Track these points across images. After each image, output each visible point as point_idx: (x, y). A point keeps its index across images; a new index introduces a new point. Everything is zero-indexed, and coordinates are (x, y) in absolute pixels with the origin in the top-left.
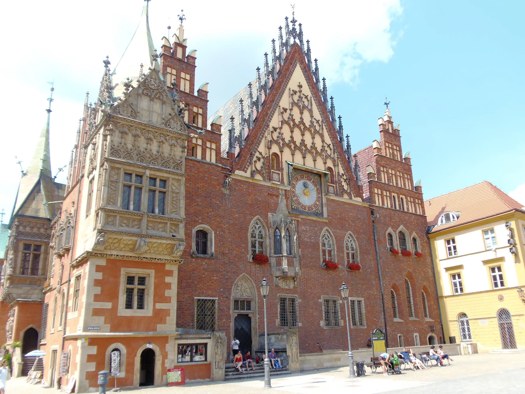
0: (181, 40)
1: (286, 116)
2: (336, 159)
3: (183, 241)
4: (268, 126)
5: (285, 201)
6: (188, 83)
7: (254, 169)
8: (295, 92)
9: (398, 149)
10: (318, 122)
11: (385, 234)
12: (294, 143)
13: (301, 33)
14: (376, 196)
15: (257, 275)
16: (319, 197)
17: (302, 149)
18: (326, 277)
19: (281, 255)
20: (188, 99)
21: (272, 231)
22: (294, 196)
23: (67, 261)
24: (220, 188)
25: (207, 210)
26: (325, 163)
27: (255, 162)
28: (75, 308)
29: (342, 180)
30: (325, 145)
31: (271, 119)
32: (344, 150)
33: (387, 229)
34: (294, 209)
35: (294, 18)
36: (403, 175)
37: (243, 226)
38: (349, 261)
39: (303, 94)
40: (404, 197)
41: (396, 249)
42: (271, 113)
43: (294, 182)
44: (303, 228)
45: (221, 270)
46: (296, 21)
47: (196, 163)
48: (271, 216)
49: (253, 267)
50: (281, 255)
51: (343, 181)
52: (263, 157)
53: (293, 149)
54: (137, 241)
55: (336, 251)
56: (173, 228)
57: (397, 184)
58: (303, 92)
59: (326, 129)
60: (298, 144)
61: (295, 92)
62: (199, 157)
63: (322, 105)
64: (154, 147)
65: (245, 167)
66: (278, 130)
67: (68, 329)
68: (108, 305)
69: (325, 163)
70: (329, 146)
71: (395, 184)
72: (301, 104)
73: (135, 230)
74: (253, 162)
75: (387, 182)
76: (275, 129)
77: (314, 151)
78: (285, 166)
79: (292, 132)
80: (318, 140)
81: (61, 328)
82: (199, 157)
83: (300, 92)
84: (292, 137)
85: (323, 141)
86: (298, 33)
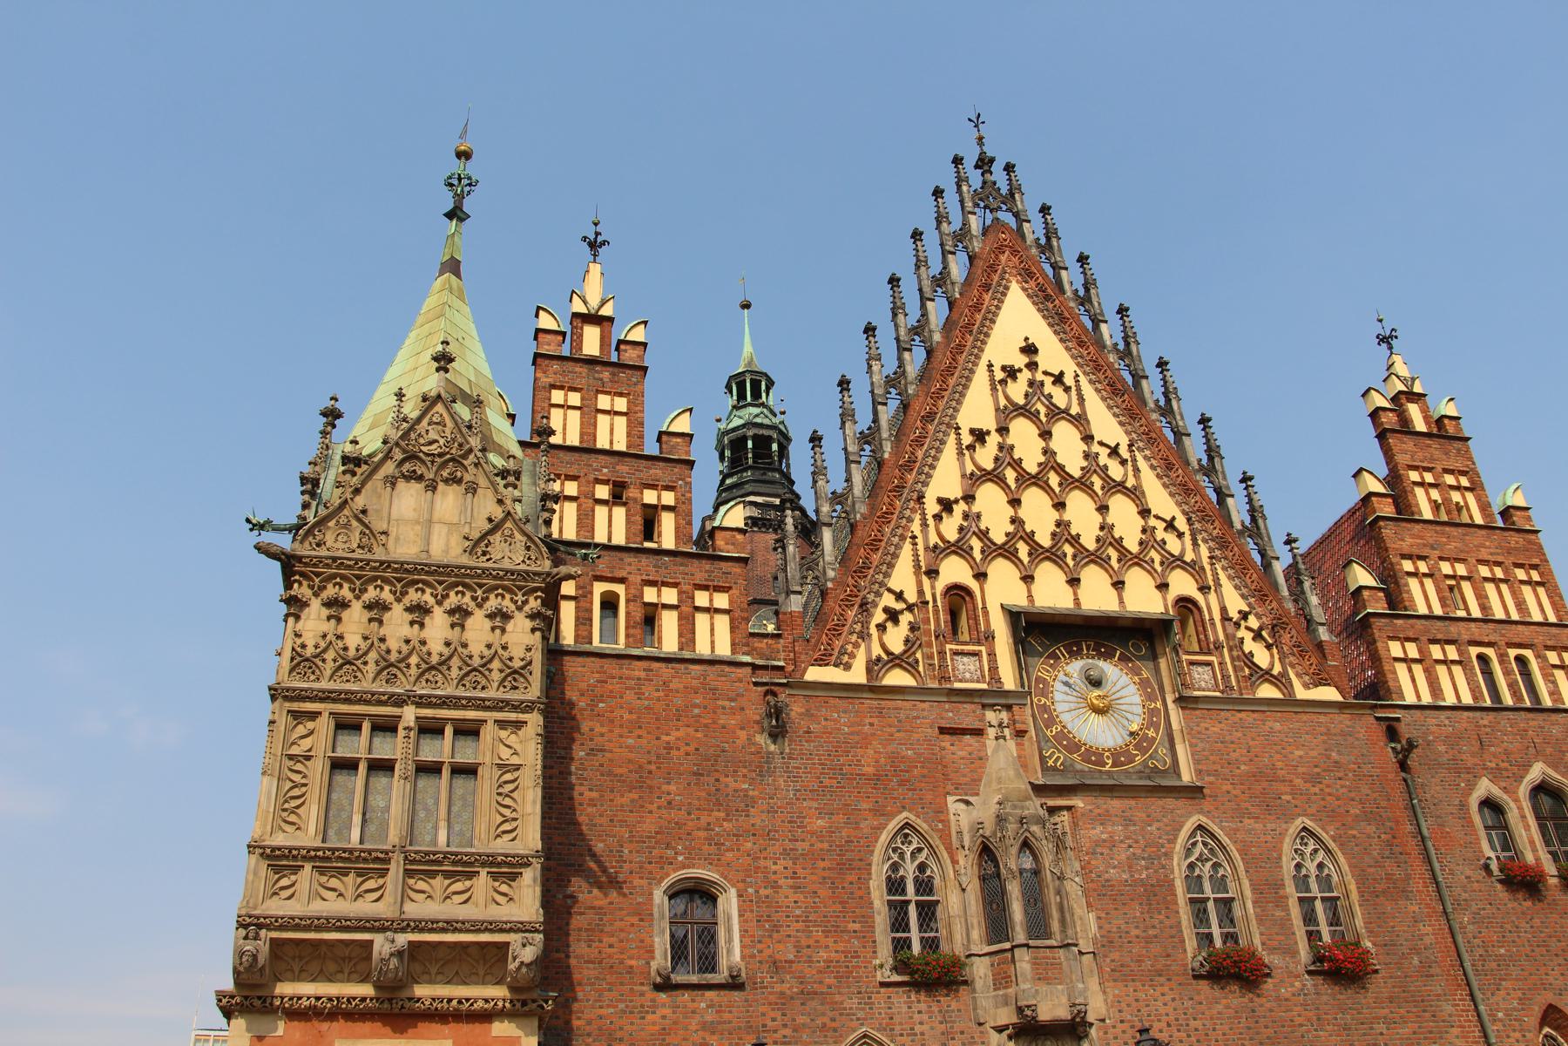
2: (1208, 567)
3: (537, 931)
4: (920, 499)
5: (1011, 744)
6: (621, 422)
7: (877, 651)
8: (1012, 373)
10: (1114, 452)
11: (1463, 806)
12: (1029, 538)
14: (1401, 669)
15: (918, 1029)
16: (1153, 712)
17: (1063, 550)
18: (1220, 1007)
19: (1007, 945)
20: (624, 470)
21: (967, 862)
25: (704, 820)
26: (1163, 587)
27: (882, 628)
29: (1242, 633)
31: (929, 476)
32: (1238, 526)
33: (1471, 787)
34: (1054, 769)
36: (1506, 571)
37: (849, 855)
38: (1313, 936)
39: (1045, 373)
41: (1530, 858)
42: (926, 456)
44: (1098, 832)
45: (770, 1024)
46: (992, 160)
47: (656, 665)
48: (962, 806)
49: (900, 998)
50: (1007, 945)
51: (1248, 636)
52: (910, 608)
53: (1026, 559)
54: (371, 942)
55: (1249, 905)
57: (1484, 607)
58: (1041, 368)
59: (1153, 467)
60: (1044, 540)
61: (1012, 373)
63: (1125, 396)
64: (438, 628)
65: (843, 652)
66: (959, 509)
69: (1163, 587)
70: (1170, 525)
71: (1476, 612)
73: (366, 907)
74: (873, 630)
76: (947, 505)
79: (1015, 502)
80: (1123, 514)
82: (669, 641)
83: (1032, 366)
84: (1014, 520)
85: (1145, 512)
86: (1004, 191)
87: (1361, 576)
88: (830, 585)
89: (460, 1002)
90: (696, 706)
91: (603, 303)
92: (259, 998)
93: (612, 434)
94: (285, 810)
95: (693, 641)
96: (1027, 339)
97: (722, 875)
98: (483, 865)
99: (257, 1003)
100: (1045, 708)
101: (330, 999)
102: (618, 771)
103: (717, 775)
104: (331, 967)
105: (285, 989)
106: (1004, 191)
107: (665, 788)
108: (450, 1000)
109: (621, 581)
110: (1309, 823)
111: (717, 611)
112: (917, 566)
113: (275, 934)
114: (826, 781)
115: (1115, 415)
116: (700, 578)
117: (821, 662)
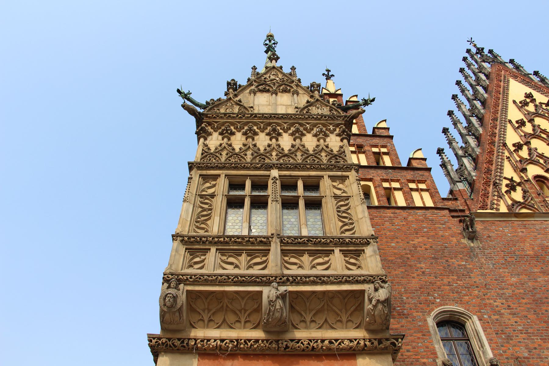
4: (505, 145)
24: (459, 242)
25: (446, 281)
56: (352, 261)
88: (474, 178)
89: (330, 342)
90: (425, 228)
92: (179, 339)
94: (197, 222)
97: (465, 309)
98: (336, 245)
99: (177, 343)
101: (231, 341)
102: (390, 258)
103: (446, 258)
104: (231, 318)
105: (199, 333)
107: (418, 265)
108: (323, 341)
109: (370, 180)
111: (422, 190)
113: (190, 288)
114: (509, 259)
116: (409, 177)
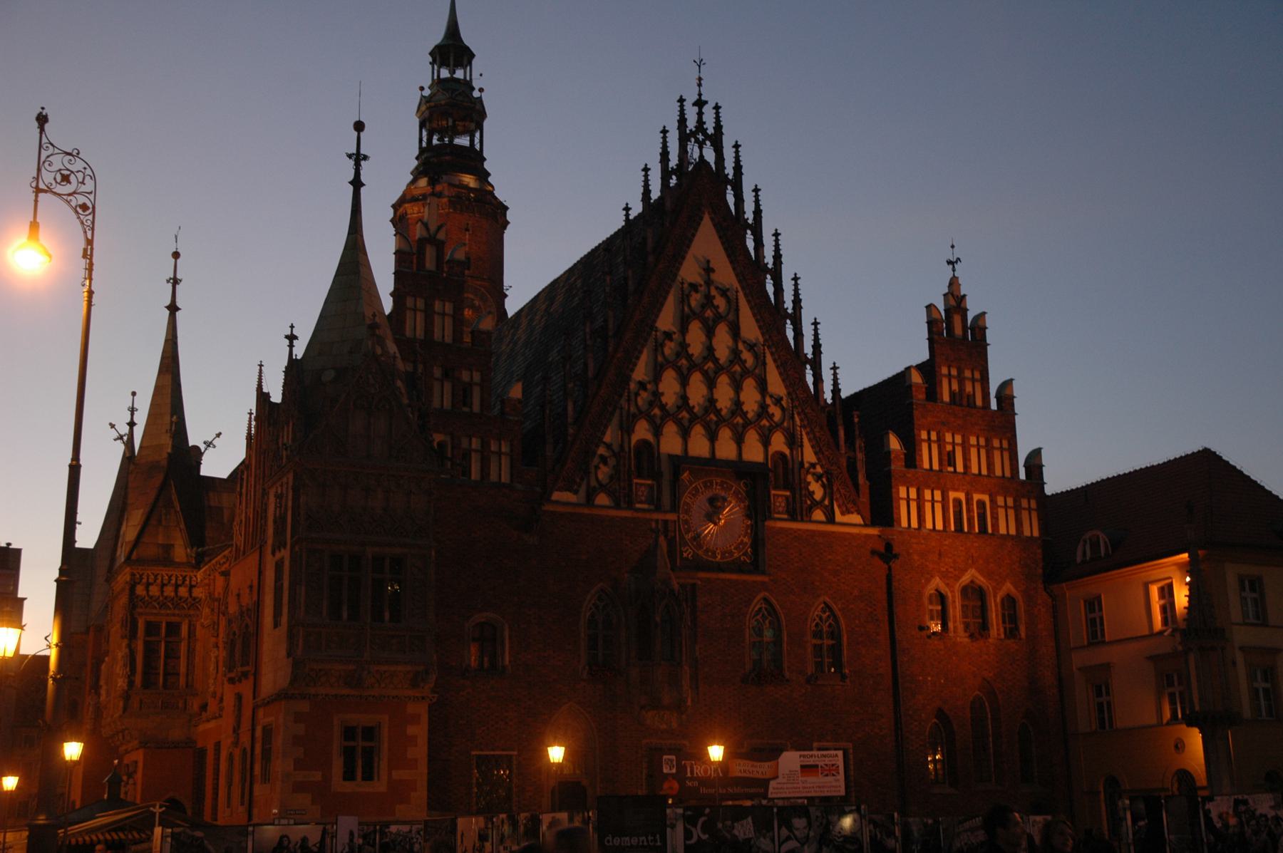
0: (433, 228)
1: (670, 349)
4: (629, 378)
6: (448, 322)
7: (593, 483)
8: (694, 287)
9: (977, 375)
10: (751, 347)
13: (718, 127)
17: (711, 420)
22: (688, 531)
23: (246, 688)
28: (266, 778)
29: (810, 478)
30: (768, 401)
32: (822, 403)
33: (928, 581)
34: (687, 559)
35: (700, 95)
36: (987, 440)
40: (986, 498)
43: (688, 500)
46: (706, 102)
57: (967, 466)
59: (775, 361)
62: (475, 474)
67: (255, 811)
68: (317, 776)
70: (778, 401)
71: (960, 468)
72: (709, 313)
74: (593, 470)
75: (936, 466)
76: (642, 385)
77: (739, 420)
78: (665, 467)
81: (241, 809)
82: (475, 474)
83: (709, 283)
86: (711, 131)
87: (894, 443)
91: (440, 228)
93: (444, 331)
95: (489, 474)
96: (708, 262)
100: (686, 522)
106: (711, 131)
110: (827, 600)
112: (621, 428)
115: (757, 321)
117: (560, 490)
